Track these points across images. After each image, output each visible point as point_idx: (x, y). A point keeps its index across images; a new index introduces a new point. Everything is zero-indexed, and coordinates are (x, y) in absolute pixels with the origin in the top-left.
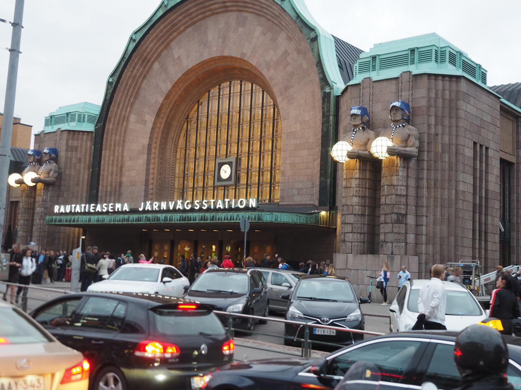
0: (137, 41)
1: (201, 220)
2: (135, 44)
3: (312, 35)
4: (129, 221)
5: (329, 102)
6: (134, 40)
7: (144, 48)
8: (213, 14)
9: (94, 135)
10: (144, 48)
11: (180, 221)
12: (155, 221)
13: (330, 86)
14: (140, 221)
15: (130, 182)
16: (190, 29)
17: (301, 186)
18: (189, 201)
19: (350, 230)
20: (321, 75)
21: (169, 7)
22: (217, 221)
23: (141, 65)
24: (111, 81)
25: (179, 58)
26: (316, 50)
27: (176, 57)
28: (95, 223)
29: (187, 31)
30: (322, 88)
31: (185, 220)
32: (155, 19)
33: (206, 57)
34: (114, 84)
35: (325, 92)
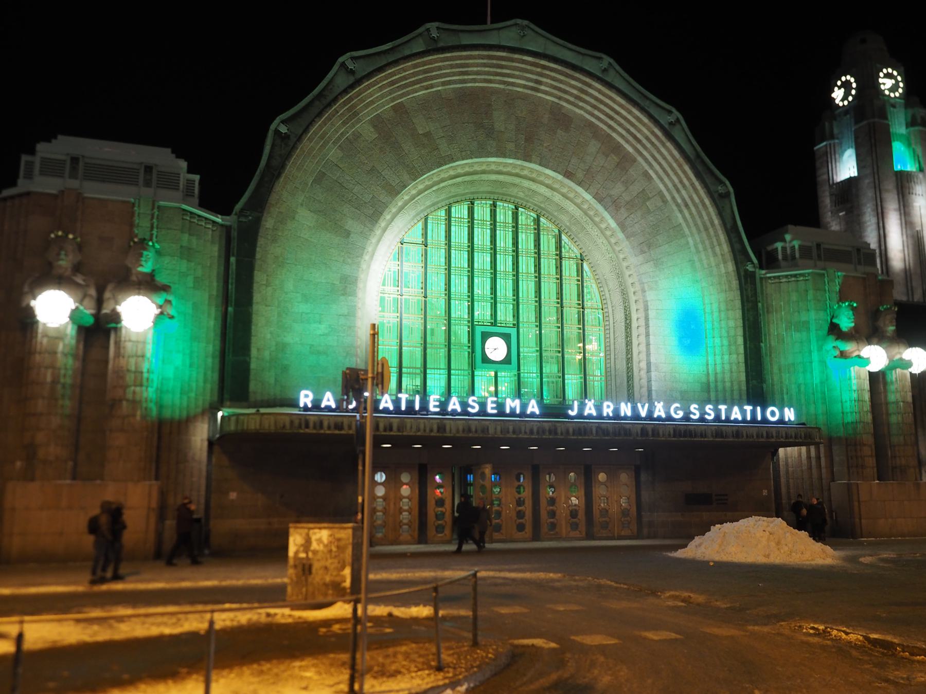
0: (358, 76)
1: (716, 437)
2: (351, 80)
3: (721, 189)
4: (556, 433)
5: (754, 283)
6: (352, 72)
9: (234, 234)
11: (674, 437)
12: (620, 434)
13: (753, 263)
14: (585, 434)
15: (311, 346)
18: (678, 405)
19: (870, 453)
20: (737, 246)
21: (441, 44)
22: (744, 439)
25: (428, 135)
27: (421, 132)
28: (460, 435)
31: (685, 436)
35: (746, 271)
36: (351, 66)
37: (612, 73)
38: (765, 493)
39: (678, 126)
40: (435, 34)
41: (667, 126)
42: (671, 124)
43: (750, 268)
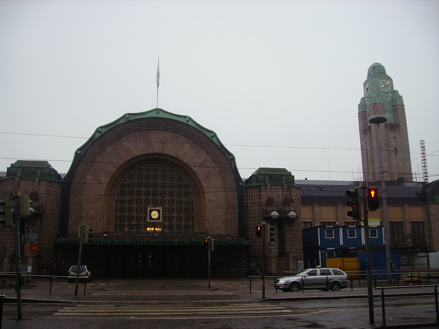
0: (103, 133)
2: (100, 134)
3: (231, 157)
6: (100, 132)
7: (105, 137)
8: (155, 129)
10: (105, 137)
16: (137, 133)
17: (218, 226)
20: (236, 177)
21: (130, 119)
23: (99, 147)
24: (79, 152)
25: (128, 148)
26: (233, 165)
29: (134, 134)
30: (237, 183)
32: (118, 123)
33: (150, 151)
34: (82, 155)
36: (100, 130)
37: (190, 121)
38: (244, 261)
39: (215, 137)
40: (128, 116)
41: (210, 137)
42: (212, 136)
43: (241, 184)
